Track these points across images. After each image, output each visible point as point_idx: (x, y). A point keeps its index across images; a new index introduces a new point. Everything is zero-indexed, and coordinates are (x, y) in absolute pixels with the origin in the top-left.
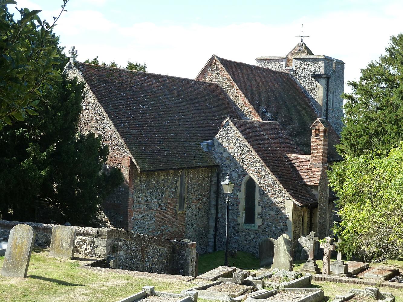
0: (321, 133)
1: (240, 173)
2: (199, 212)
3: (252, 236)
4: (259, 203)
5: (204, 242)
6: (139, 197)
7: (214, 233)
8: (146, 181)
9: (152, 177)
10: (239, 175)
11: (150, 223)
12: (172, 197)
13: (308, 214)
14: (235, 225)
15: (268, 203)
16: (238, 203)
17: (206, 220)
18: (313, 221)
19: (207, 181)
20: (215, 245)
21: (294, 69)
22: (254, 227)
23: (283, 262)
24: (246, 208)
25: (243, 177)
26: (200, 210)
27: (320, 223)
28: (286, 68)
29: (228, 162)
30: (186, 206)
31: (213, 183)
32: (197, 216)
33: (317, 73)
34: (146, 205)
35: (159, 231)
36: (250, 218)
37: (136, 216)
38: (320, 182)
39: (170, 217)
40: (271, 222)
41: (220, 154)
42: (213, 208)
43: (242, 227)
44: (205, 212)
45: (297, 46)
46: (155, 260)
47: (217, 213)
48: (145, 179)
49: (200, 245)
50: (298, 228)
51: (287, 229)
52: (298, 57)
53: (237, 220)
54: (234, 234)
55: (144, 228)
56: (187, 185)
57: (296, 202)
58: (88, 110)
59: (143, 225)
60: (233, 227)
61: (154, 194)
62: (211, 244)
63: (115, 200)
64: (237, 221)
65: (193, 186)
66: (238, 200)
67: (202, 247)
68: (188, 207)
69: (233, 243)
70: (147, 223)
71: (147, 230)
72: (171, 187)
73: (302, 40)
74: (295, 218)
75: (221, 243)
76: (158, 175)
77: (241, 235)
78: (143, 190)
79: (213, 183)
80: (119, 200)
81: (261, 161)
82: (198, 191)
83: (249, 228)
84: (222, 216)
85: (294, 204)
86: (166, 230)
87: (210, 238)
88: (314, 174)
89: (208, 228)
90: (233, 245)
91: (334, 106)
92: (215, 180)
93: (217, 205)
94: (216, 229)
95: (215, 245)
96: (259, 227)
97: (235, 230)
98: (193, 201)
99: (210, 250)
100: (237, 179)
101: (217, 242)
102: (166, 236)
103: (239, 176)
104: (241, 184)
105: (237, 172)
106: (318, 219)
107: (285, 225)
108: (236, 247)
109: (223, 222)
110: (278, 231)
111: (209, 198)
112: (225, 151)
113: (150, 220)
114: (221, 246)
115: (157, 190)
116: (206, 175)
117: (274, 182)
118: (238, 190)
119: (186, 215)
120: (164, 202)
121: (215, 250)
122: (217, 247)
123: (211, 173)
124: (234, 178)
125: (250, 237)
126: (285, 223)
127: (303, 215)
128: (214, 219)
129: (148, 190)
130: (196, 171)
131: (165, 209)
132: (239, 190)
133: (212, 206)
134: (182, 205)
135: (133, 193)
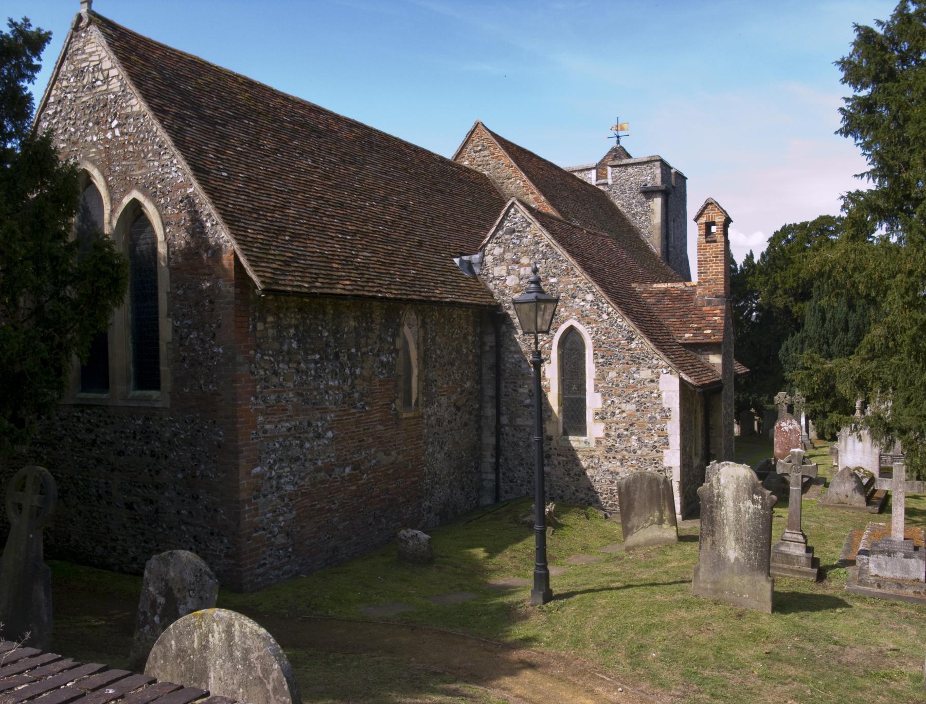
2: (456, 414)
4: (596, 386)
6: (275, 373)
7: (494, 460)
8: (296, 327)
9: (316, 318)
11: (319, 445)
12: (382, 377)
17: (475, 432)
18: (711, 423)
19: (473, 342)
20: (497, 487)
21: (610, 182)
22: (586, 442)
23: (737, 559)
26: (458, 409)
31: (487, 348)
33: (649, 185)
35: (347, 465)
37: (268, 427)
39: (380, 427)
40: (627, 430)
42: (489, 405)
44: (470, 414)
45: (610, 153)
47: (499, 414)
48: (293, 322)
49: (463, 489)
52: (616, 163)
55: (297, 459)
58: (126, 137)
59: (296, 452)
61: (329, 367)
62: (489, 485)
63: (202, 382)
65: (438, 352)
70: (307, 445)
71: (307, 464)
72: (378, 351)
73: (618, 142)
75: (511, 481)
77: (556, 462)
78: (289, 352)
79: (487, 348)
80: (211, 382)
81: (596, 288)
82: (452, 364)
84: (510, 421)
85: (683, 383)
86: (370, 461)
87: (486, 473)
92: (490, 340)
93: (497, 398)
94: (498, 451)
95: (497, 487)
96: (598, 442)
98: (441, 388)
99: (487, 500)
101: (501, 481)
102: (370, 476)
113: (319, 436)
114: (512, 488)
115: (337, 356)
116: (471, 329)
120: (358, 388)
121: (497, 499)
129: (307, 354)
130: (444, 316)
131: (363, 407)
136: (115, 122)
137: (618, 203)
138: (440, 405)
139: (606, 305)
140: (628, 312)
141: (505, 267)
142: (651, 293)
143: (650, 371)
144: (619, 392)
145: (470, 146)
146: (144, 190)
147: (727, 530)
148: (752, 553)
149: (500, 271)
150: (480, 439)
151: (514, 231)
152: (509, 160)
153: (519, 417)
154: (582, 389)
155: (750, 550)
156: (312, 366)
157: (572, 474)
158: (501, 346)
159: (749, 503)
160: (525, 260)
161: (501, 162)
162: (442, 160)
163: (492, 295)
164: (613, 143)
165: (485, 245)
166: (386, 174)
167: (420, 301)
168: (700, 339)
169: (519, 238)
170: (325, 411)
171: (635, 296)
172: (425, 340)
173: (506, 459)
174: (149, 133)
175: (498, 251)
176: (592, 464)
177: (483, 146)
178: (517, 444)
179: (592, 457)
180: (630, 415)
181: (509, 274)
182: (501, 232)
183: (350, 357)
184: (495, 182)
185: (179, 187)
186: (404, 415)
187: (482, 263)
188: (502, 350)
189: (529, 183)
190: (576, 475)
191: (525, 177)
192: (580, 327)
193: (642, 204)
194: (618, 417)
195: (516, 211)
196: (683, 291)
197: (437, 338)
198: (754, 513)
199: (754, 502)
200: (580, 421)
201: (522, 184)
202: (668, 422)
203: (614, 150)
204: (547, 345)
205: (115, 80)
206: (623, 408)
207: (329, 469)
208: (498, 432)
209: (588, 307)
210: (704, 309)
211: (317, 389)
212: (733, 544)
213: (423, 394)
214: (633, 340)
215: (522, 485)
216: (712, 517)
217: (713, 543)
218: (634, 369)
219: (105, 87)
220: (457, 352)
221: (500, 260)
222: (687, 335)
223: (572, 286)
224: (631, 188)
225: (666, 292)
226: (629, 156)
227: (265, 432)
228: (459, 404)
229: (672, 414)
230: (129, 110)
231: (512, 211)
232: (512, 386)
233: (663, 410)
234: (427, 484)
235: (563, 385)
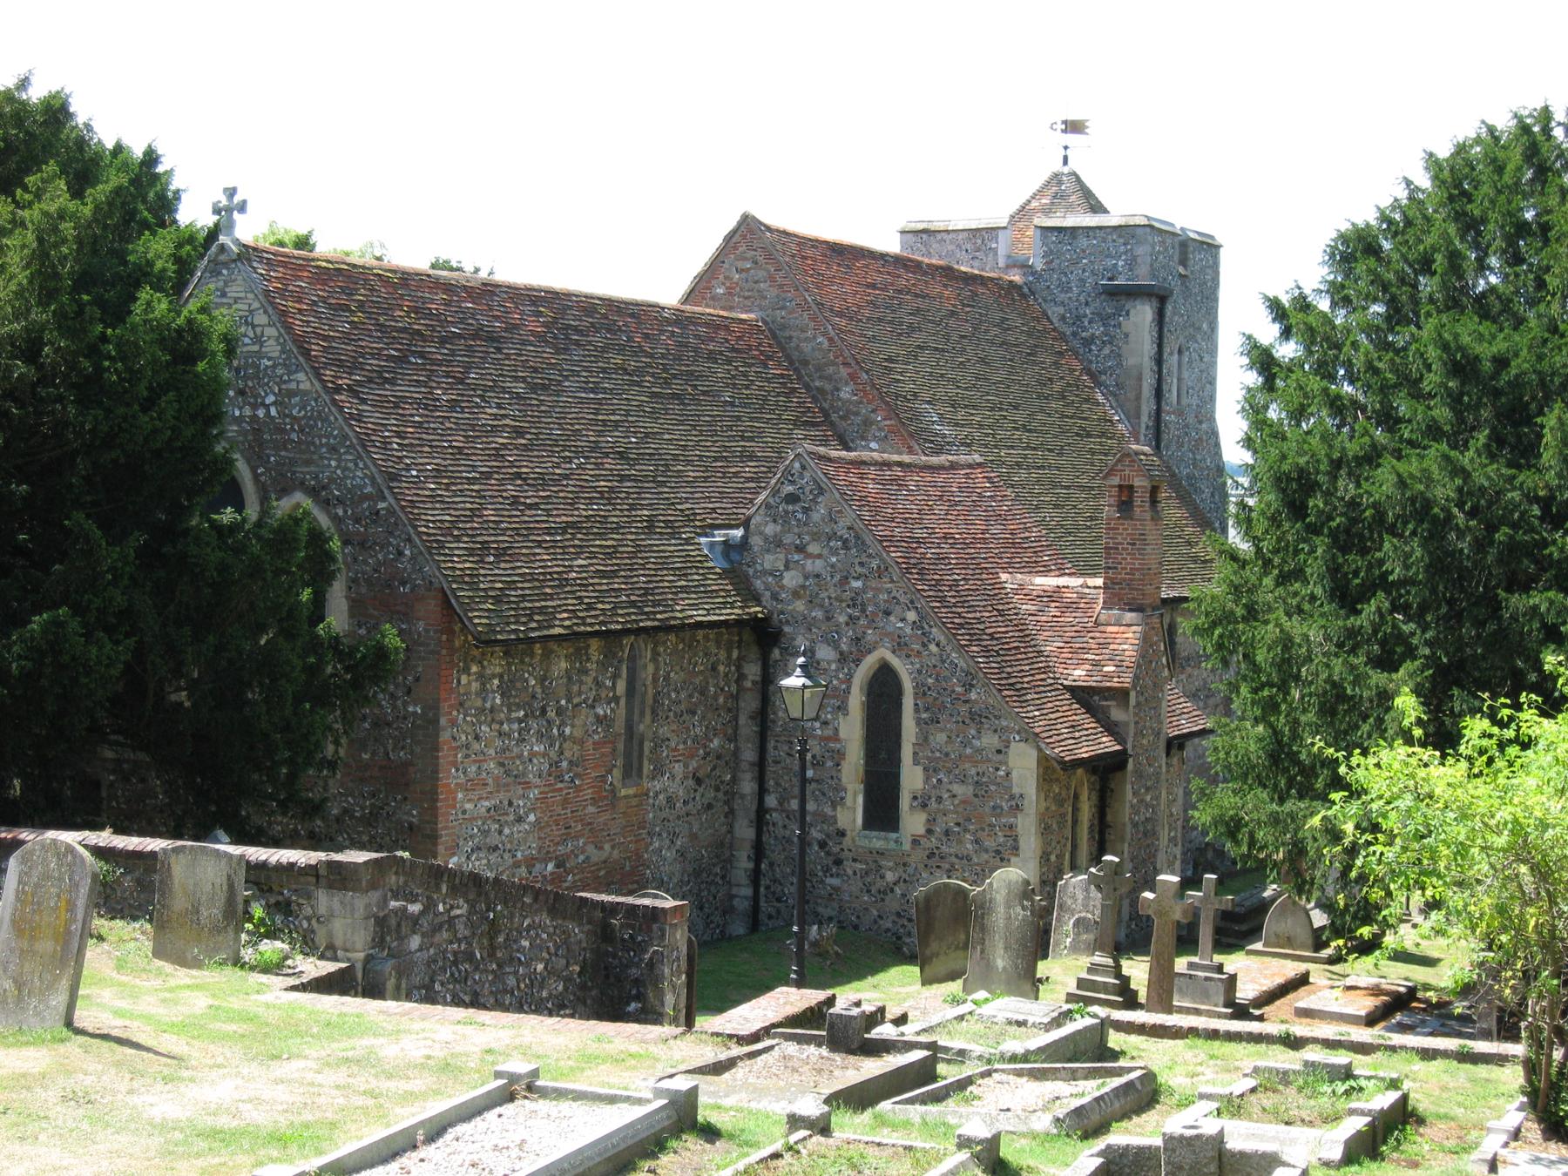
1: (844, 647)
3: (890, 877)
6: (477, 738)
7: (751, 865)
8: (501, 676)
10: (841, 653)
14: (828, 836)
15: (947, 755)
16: (839, 756)
18: (1109, 818)
19: (726, 675)
24: (867, 772)
25: (857, 662)
26: (699, 781)
27: (1135, 825)
29: (800, 606)
30: (647, 767)
31: (748, 684)
32: (690, 806)
34: (502, 765)
35: (550, 859)
36: (882, 808)
37: (468, 806)
38: (1136, 677)
39: (591, 809)
40: (958, 824)
42: (748, 776)
44: (717, 789)
45: (1047, 184)
46: (540, 967)
47: (762, 791)
48: (498, 670)
51: (1017, 849)
53: (835, 817)
54: (826, 870)
55: (496, 848)
56: (651, 691)
59: (494, 839)
60: (822, 845)
62: (742, 905)
68: (658, 772)
70: (507, 831)
71: (506, 856)
74: (1047, 809)
75: (779, 900)
76: (547, 655)
77: (850, 872)
78: (492, 710)
79: (748, 684)
80: (403, 748)
82: (694, 713)
83: (878, 844)
84: (781, 804)
86: (577, 856)
89: (731, 846)
90: (820, 909)
91: (1184, 401)
92: (753, 671)
93: (761, 765)
96: (915, 842)
97: (828, 854)
99: (738, 928)
100: (833, 666)
101: (762, 899)
103: (843, 658)
104: (849, 688)
105: (835, 644)
106: (1128, 810)
108: (833, 913)
110: (986, 856)
111: (733, 738)
113: (519, 820)
114: (778, 912)
115: (544, 711)
116: (723, 655)
120: (567, 754)
121: (754, 925)
122: (762, 916)
123: (739, 647)
124: (824, 665)
125: (883, 877)
126: (1011, 827)
127: (1076, 797)
128: (753, 816)
129: (510, 710)
130: (683, 640)
132: (842, 708)
133: (745, 766)
134: (635, 765)
135: (453, 723)
136: (270, 399)
138: (673, 777)
139: (934, 630)
141: (782, 556)
146: (313, 492)
149: (771, 561)
154: (895, 761)
156: (516, 726)
159: (1019, 909)
160: (813, 548)
166: (592, 391)
167: (653, 628)
169: (806, 510)
170: (528, 785)
171: (999, 601)
174: (323, 421)
176: (905, 876)
177: (756, 263)
180: (964, 802)
181: (787, 568)
183: (560, 711)
185: (368, 497)
186: (623, 792)
192: (896, 662)
199: (1024, 908)
201: (826, 343)
203: (1056, 178)
205: (272, 342)
207: (530, 862)
208: (760, 818)
209: (908, 630)
211: (520, 756)
214: (972, 686)
217: (982, 951)
218: (973, 732)
219: (256, 348)
220: (702, 693)
221: (777, 543)
224: (1082, 281)
225: (1054, 595)
227: (464, 812)
228: (700, 774)
230: (293, 386)
233: (1012, 797)
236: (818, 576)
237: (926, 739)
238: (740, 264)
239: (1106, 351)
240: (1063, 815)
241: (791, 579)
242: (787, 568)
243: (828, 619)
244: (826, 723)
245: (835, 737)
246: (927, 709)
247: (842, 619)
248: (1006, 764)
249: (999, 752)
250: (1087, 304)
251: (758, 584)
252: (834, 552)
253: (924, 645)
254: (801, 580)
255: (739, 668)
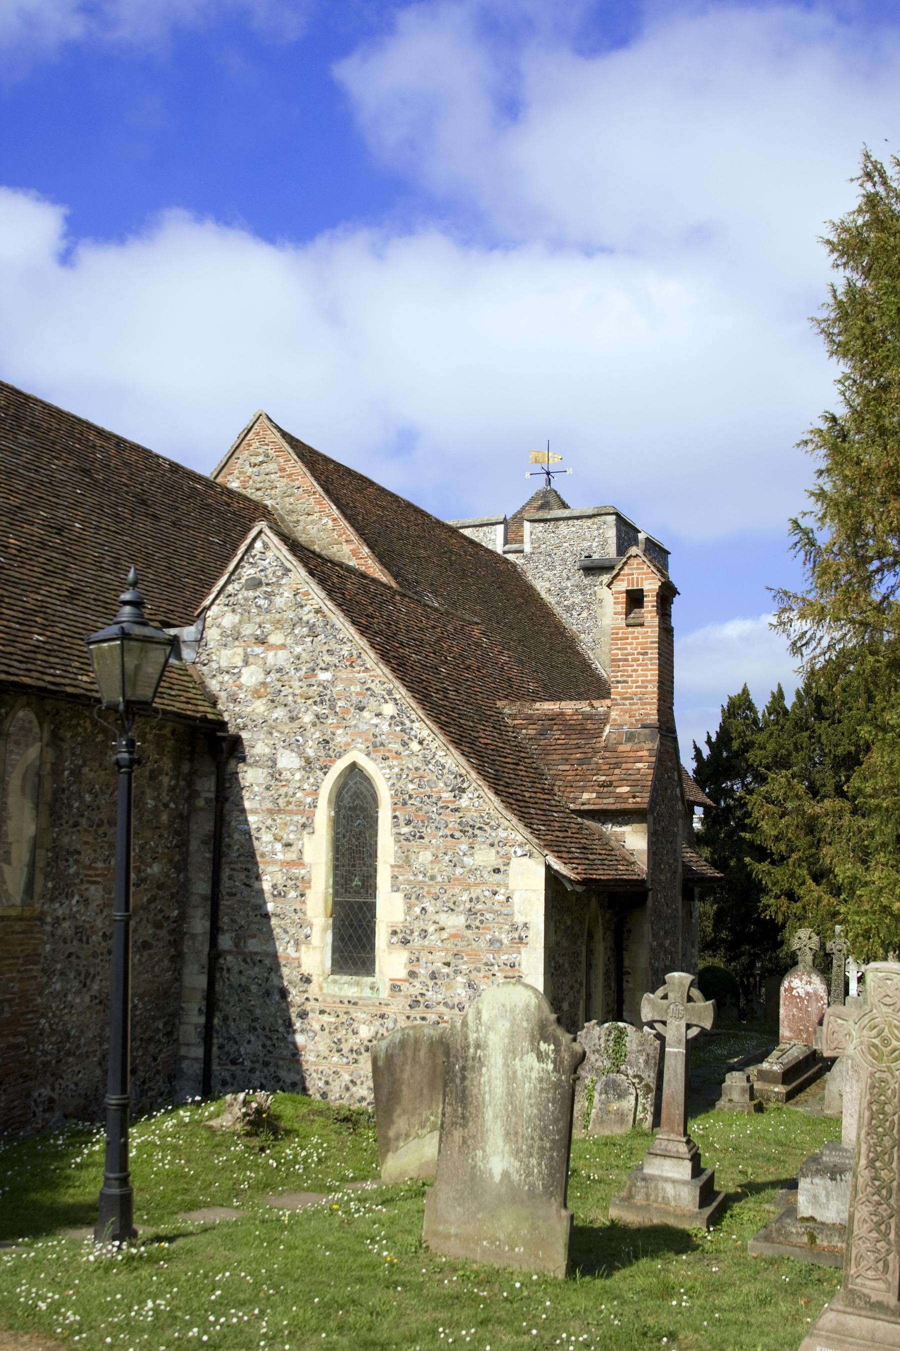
0: (650, 602)
1: (310, 753)
4: (395, 877)
5: (155, 1059)
7: (202, 1020)
10: (308, 761)
13: (608, 933)
15: (433, 878)
17: (166, 963)
18: (626, 962)
19: (172, 789)
22: (372, 988)
23: (506, 1175)
24: (335, 904)
25: (325, 769)
28: (508, 547)
33: (595, 556)
38: (653, 801)
40: (448, 964)
41: (227, 677)
42: (199, 912)
43: (321, 989)
44: (158, 926)
47: (215, 931)
50: (572, 988)
53: (298, 959)
57: (557, 865)
64: (299, 966)
66: (303, 872)
67: (144, 1083)
69: (281, 1063)
74: (558, 944)
75: (234, 1062)
79: (201, 803)
81: (401, 693)
84: (237, 945)
85: (552, 878)
87: (188, 1045)
88: (629, 766)
89: (178, 997)
92: (207, 787)
93: (214, 899)
96: (395, 988)
98: (89, 867)
100: (298, 776)
101: (215, 1061)
104: (315, 801)
105: (297, 748)
107: (510, 974)
109: (241, 972)
111: (182, 866)
112: (251, 660)
114: (233, 1076)
116: (167, 763)
117: (459, 780)
118: (304, 826)
119: (48, 928)
124: (286, 775)
125: (355, 1033)
126: (513, 966)
127: (591, 936)
128: (204, 960)
133: (195, 900)
137: (541, 586)
139: (416, 725)
140: (460, 737)
141: (240, 651)
142: (529, 718)
143: (493, 851)
144: (435, 890)
145: (243, 454)
147: (489, 1114)
148: (534, 1161)
149: (229, 657)
150: (178, 979)
151: (260, 584)
152: (308, 481)
153: (254, 936)
154: (369, 885)
155: (531, 1155)
157: (345, 1048)
158: (227, 799)
159: (531, 1059)
160: (276, 638)
161: (297, 483)
162: (199, 478)
163: (214, 704)
164: (540, 484)
165: (208, 608)
167: (40, 689)
168: (609, 803)
169: (268, 596)
172: (56, 771)
173: (225, 1019)
175: (229, 620)
177: (267, 456)
178: (245, 989)
179: (382, 1016)
180: (454, 936)
181: (246, 663)
182: (236, 586)
184: (283, 520)
187: (200, 640)
188: (228, 806)
189: (343, 523)
190: (352, 1051)
191: (336, 512)
192: (370, 766)
193: (582, 589)
194: (433, 939)
195: (266, 546)
196: (588, 717)
197: (86, 770)
198: (541, 1080)
199: (541, 1057)
200: (364, 947)
201: (330, 523)
202: (523, 950)
204: (309, 800)
206: (442, 924)
209: (385, 727)
210: (621, 748)
212: (500, 1142)
213: (47, 876)
214: (463, 791)
215: (252, 1071)
216: (464, 1090)
218: (464, 847)
222: (586, 796)
223: (358, 689)
225: (554, 718)
226: (565, 506)
229: (531, 934)
231: (258, 545)
232: (242, 876)
234: (45, 1053)
235: (335, 876)
236: (280, 670)
237: (407, 860)
238: (254, 460)
239: (585, 614)
240: (577, 954)
241: (251, 677)
242: (246, 663)
243: (292, 719)
244: (288, 845)
245: (299, 862)
246: (408, 823)
247: (307, 718)
248: (506, 886)
249: (497, 871)
250: (568, 579)
251: (213, 685)
252: (300, 640)
253: (405, 744)
254: (261, 677)
255: (190, 784)
